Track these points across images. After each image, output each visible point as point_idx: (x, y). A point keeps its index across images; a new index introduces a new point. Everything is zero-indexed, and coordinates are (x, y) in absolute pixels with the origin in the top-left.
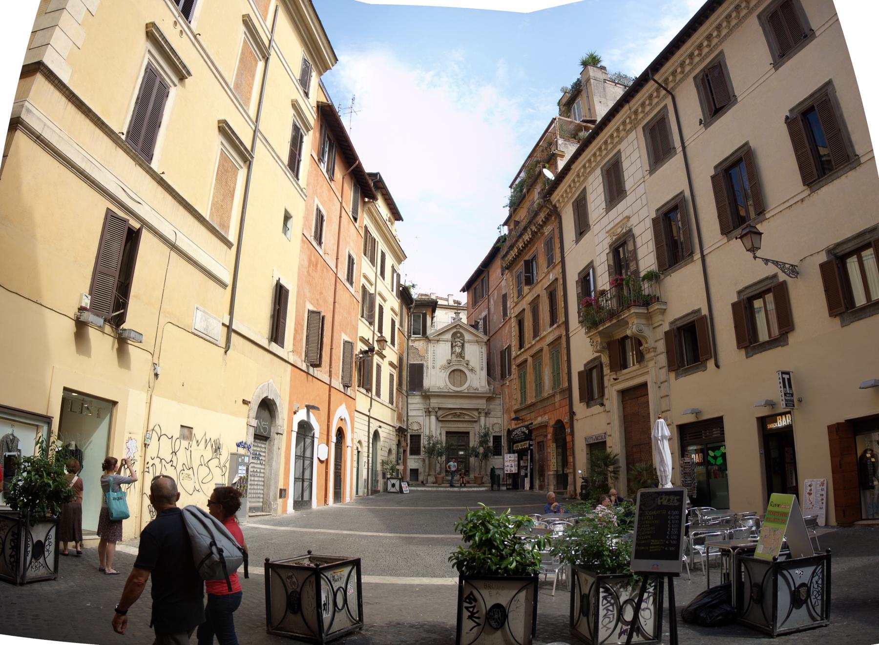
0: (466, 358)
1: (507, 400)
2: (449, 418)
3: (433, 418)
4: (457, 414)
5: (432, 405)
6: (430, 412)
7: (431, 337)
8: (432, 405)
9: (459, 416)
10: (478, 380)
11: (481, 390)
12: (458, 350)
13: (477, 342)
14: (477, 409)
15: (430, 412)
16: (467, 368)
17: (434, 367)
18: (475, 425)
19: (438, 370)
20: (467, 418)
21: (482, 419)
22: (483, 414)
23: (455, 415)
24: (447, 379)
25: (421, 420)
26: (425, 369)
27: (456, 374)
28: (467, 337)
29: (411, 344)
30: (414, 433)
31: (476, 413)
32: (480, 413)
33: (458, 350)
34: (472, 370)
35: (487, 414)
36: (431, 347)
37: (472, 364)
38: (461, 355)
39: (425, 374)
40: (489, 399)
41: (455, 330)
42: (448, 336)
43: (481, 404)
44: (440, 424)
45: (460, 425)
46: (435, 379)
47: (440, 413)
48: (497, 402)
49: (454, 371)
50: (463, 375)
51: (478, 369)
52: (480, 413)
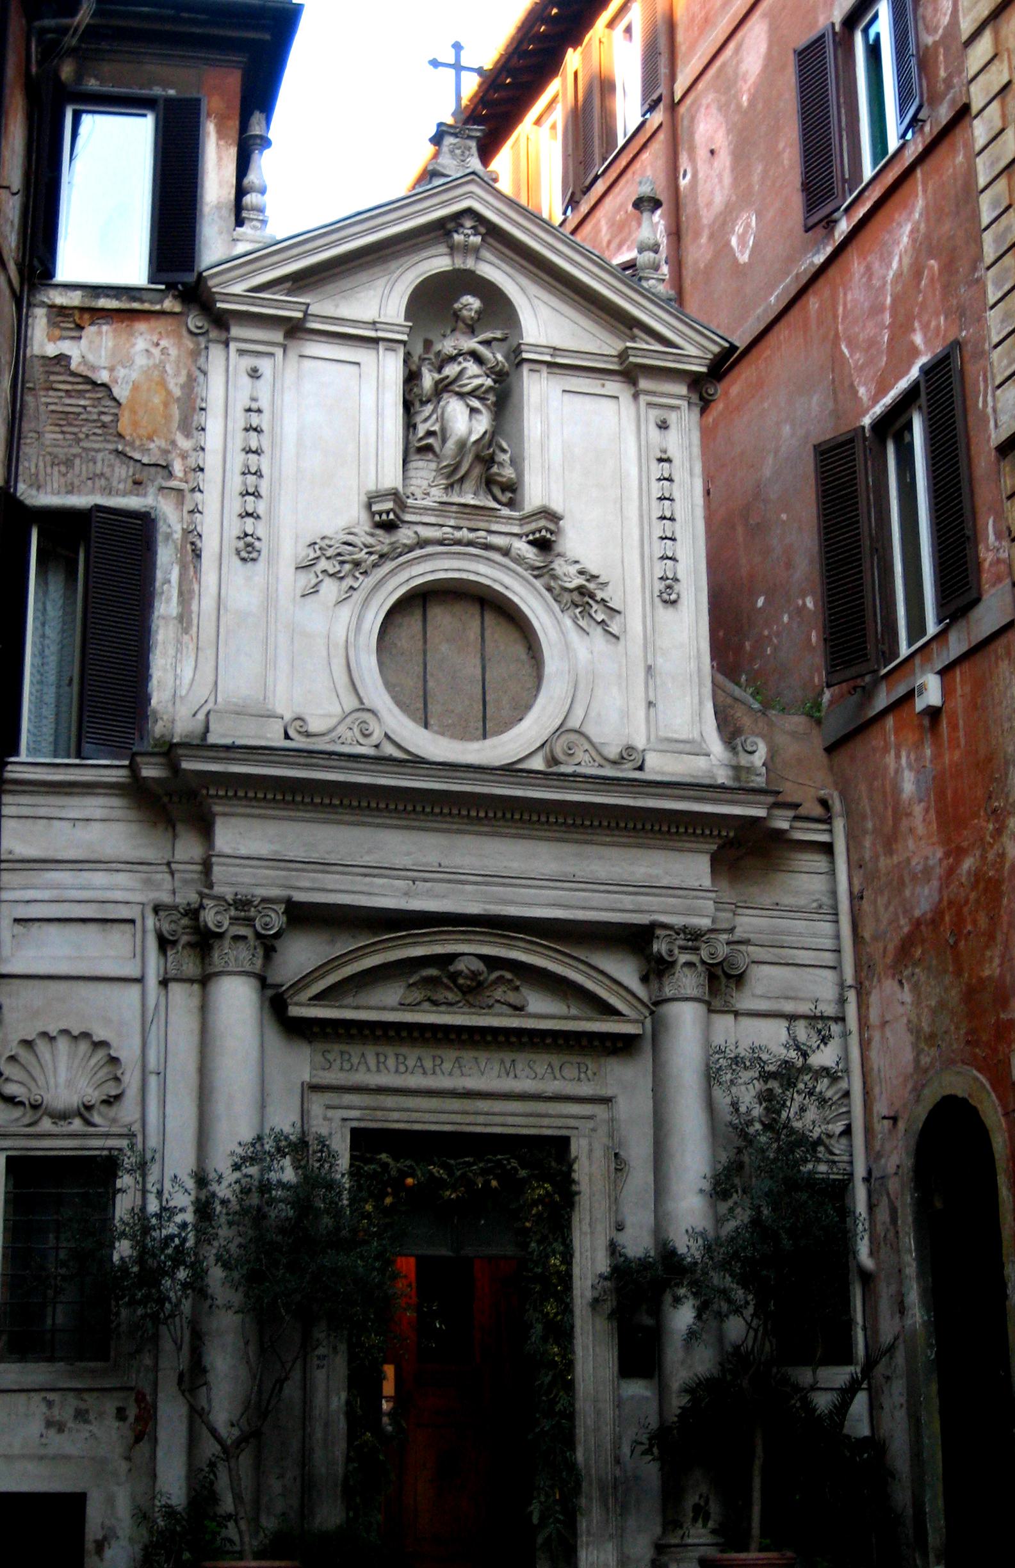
0: (534, 495)
1: (921, 847)
2: (386, 1004)
3: (237, 998)
4: (454, 972)
5: (230, 880)
6: (204, 942)
7: (233, 290)
8: (230, 880)
9: (472, 990)
10: (636, 688)
11: (659, 766)
12: (463, 422)
13: (630, 373)
14: (634, 939)
15: (204, 942)
16: (539, 572)
17: (248, 550)
18: (625, 1080)
19: (289, 581)
20: (542, 1010)
21: (686, 1021)
22: (688, 982)
23: (437, 977)
24: (368, 663)
25: (117, 1015)
26: (166, 558)
27: (456, 619)
28: (543, 321)
29: (43, 342)
30: (58, 1141)
31: (624, 970)
32: (657, 969)
33: (463, 422)
34: (584, 599)
35: (723, 981)
36: (225, 379)
37: (583, 546)
38: (489, 470)
39: (166, 607)
40: (746, 849)
41: (438, 262)
42: (383, 300)
43: (673, 885)
44: (300, 1063)
45: (485, 1073)
46: (262, 646)
47: (301, 955)
48: (805, 881)
49: (420, 600)
50: (500, 637)
51: (628, 588)
52: (657, 969)
